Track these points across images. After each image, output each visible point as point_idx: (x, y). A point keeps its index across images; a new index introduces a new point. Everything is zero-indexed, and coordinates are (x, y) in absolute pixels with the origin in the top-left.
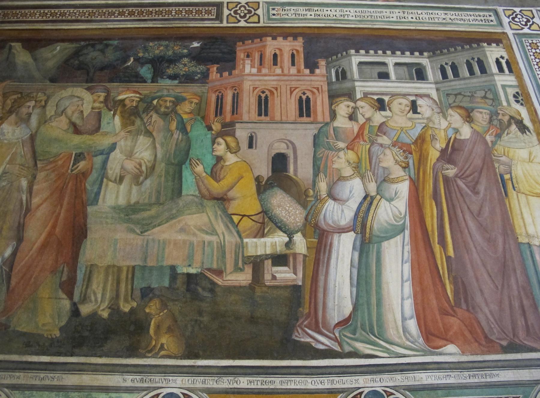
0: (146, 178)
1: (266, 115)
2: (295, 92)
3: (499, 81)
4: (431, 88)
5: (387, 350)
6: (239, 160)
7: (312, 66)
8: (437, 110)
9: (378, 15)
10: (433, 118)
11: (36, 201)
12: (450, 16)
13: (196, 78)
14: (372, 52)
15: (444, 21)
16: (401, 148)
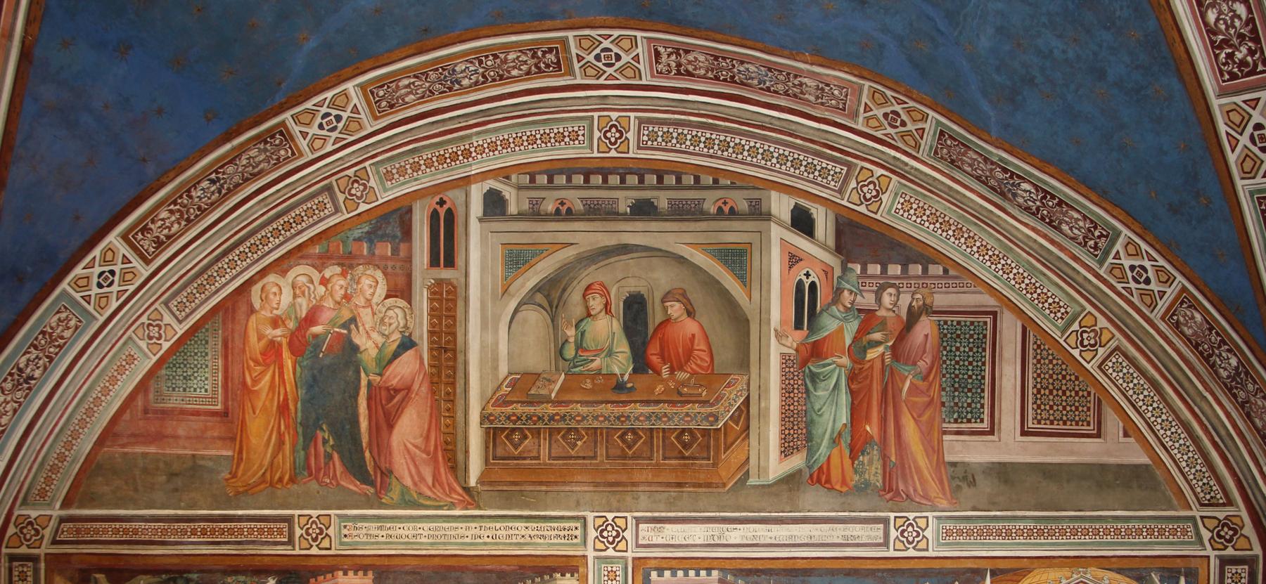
9: (453, 533)
15: (522, 541)
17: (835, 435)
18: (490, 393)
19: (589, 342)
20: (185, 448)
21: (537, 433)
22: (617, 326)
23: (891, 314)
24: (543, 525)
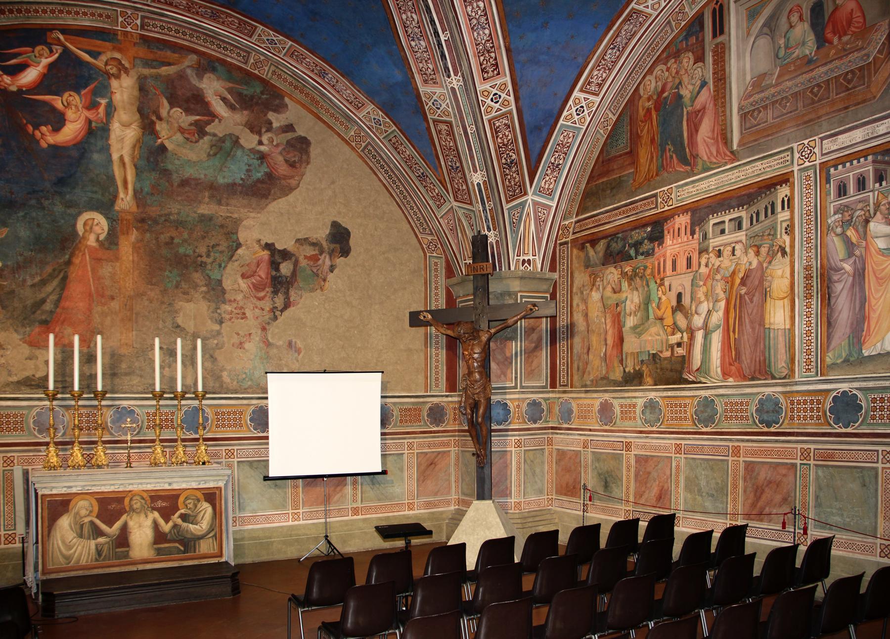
5: (710, 381)
7: (693, 233)
8: (744, 251)
11: (608, 328)
22: (806, 26)
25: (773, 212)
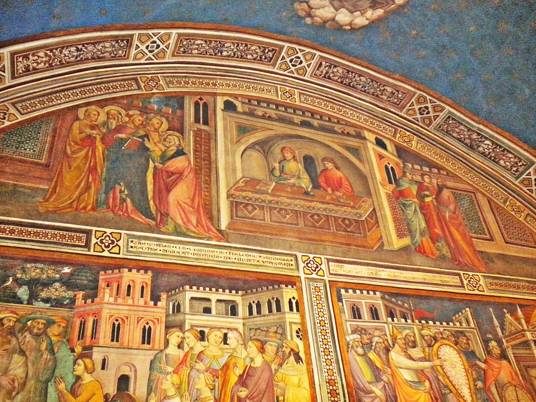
0: (18, 393)
1: (117, 341)
2: (141, 322)
3: (289, 318)
4: (239, 323)
6: (94, 379)
7: (156, 299)
9: (211, 254)
10: (237, 349)
12: (263, 259)
13: (65, 303)
14: (201, 288)
15: (258, 263)
16: (211, 373)
17: (422, 231)
18: (232, 185)
19: (286, 170)
20: (8, 179)
21: (262, 208)
22: (301, 167)
23: (429, 185)
24: (270, 256)
25: (279, 309)
